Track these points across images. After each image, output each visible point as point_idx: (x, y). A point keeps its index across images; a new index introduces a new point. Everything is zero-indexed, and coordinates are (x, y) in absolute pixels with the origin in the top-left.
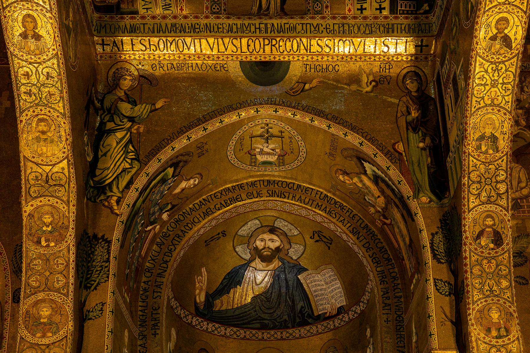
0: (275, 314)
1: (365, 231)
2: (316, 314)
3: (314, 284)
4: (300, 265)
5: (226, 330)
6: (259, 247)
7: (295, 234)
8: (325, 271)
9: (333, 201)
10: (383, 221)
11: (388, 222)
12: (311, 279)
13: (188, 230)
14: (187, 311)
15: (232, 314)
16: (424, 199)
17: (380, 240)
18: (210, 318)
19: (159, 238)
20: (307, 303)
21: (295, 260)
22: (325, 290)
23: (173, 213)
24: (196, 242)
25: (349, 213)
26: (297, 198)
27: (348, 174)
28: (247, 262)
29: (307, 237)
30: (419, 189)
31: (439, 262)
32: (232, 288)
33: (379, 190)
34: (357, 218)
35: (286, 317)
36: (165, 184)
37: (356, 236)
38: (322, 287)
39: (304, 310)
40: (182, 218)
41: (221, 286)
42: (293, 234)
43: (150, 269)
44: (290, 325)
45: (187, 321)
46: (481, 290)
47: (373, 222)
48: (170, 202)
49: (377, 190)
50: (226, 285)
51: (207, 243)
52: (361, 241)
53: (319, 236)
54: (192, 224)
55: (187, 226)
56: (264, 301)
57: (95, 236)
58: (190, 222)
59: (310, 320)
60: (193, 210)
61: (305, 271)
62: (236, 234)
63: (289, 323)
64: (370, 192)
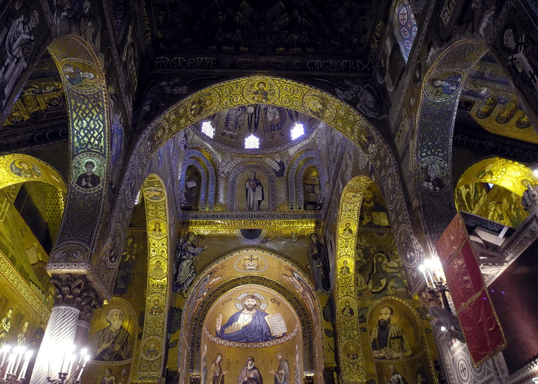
2: (272, 336)
11: (305, 297)
16: (320, 291)
22: (277, 324)
24: (218, 304)
26: (264, 284)
27: (287, 276)
29: (269, 301)
31: (327, 321)
34: (291, 294)
35: (258, 337)
44: (260, 341)
46: (345, 336)
47: (298, 296)
51: (223, 304)
57: (175, 308)
59: (270, 339)
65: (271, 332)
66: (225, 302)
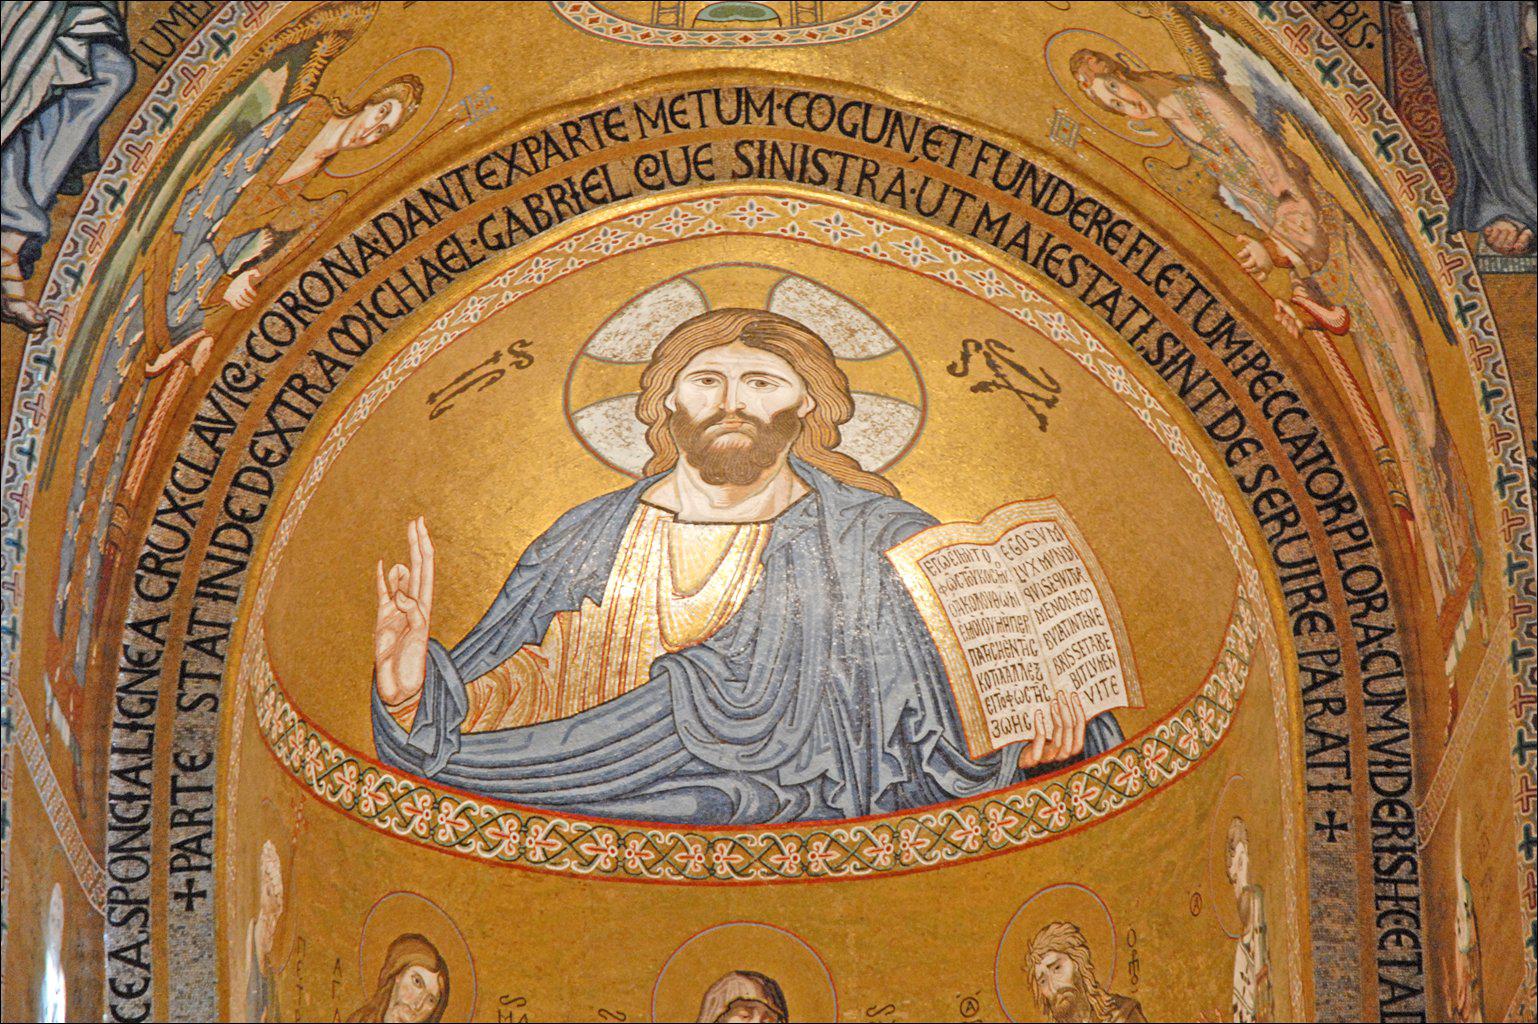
0: (773, 747)
1: (1220, 351)
3: (966, 592)
4: (897, 495)
5: (524, 830)
6: (692, 412)
7: (876, 349)
8: (1023, 529)
9: (1061, 200)
10: (1308, 311)
11: (1333, 317)
12: (953, 570)
13: (351, 353)
14: (336, 743)
15: (557, 749)
17: (1295, 398)
18: (444, 771)
19: (209, 397)
20: (932, 690)
21: (875, 474)
22: (1023, 623)
23: (275, 271)
25: (1143, 257)
28: (630, 482)
30: (1478, 181)
32: (555, 614)
33: (1285, 164)
34: (1180, 284)
35: (827, 762)
36: (243, 146)
37: (1177, 381)
38: (1009, 611)
39: (920, 724)
40: (319, 293)
41: (504, 608)
42: (864, 350)
43: (163, 556)
45: (334, 794)
48: (262, 222)
49: (1277, 162)
50: (527, 600)
52: (1201, 404)
53: (992, 365)
54: (372, 325)
55: (346, 331)
56: (718, 675)
58: (356, 311)
60: (375, 251)
61: (925, 528)
62: (582, 352)
63: (843, 789)
64: (1242, 168)
65: (966, 715)
66: (464, 382)
